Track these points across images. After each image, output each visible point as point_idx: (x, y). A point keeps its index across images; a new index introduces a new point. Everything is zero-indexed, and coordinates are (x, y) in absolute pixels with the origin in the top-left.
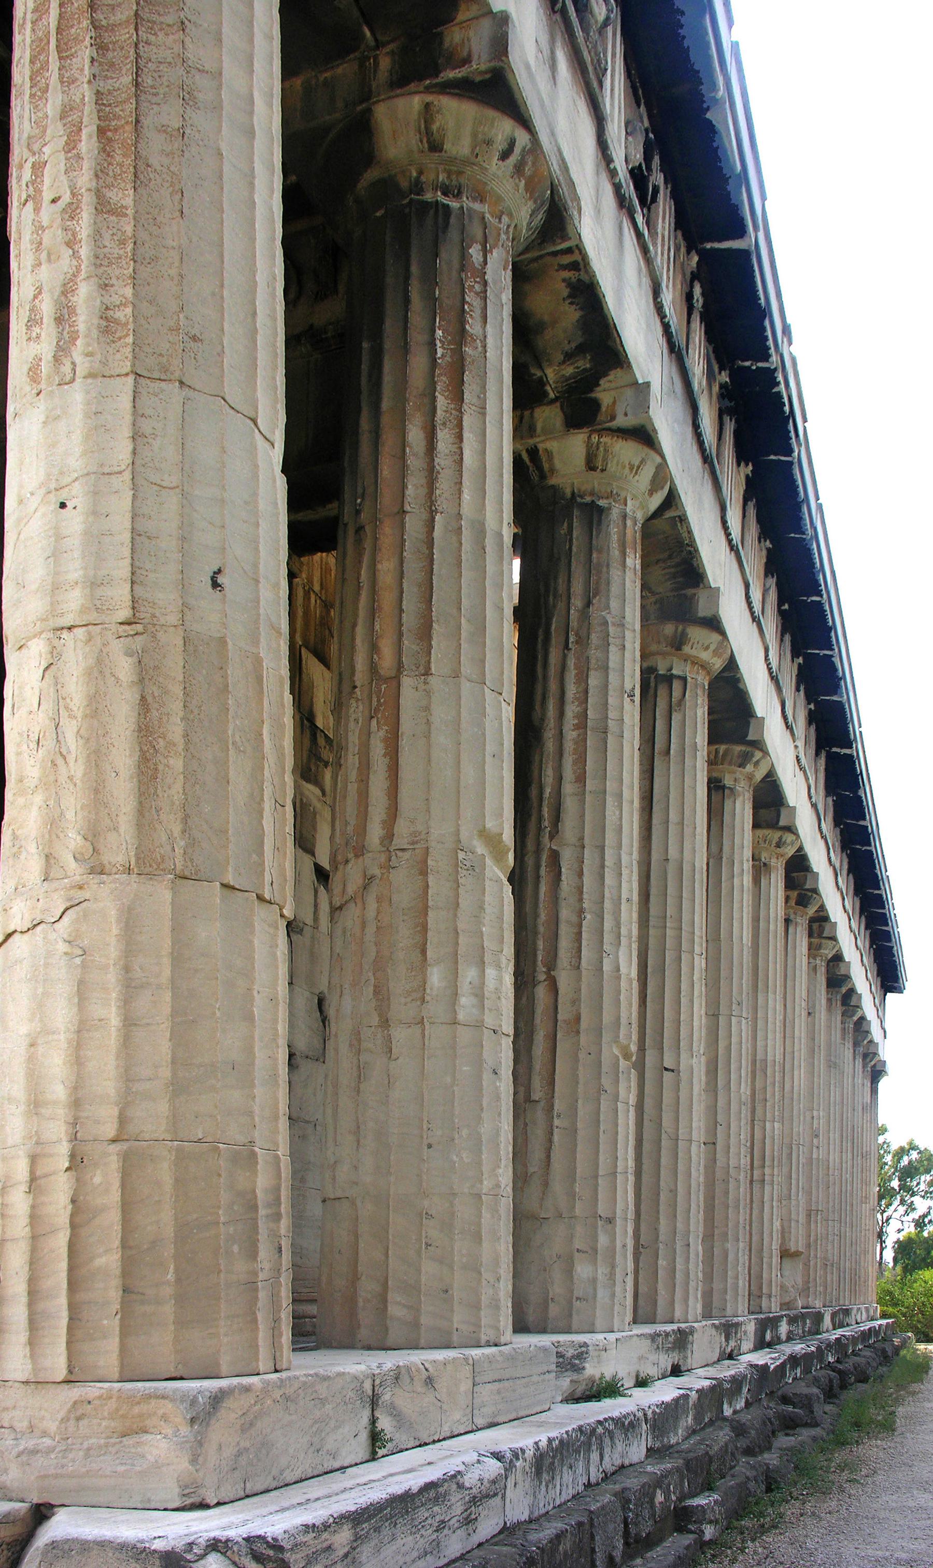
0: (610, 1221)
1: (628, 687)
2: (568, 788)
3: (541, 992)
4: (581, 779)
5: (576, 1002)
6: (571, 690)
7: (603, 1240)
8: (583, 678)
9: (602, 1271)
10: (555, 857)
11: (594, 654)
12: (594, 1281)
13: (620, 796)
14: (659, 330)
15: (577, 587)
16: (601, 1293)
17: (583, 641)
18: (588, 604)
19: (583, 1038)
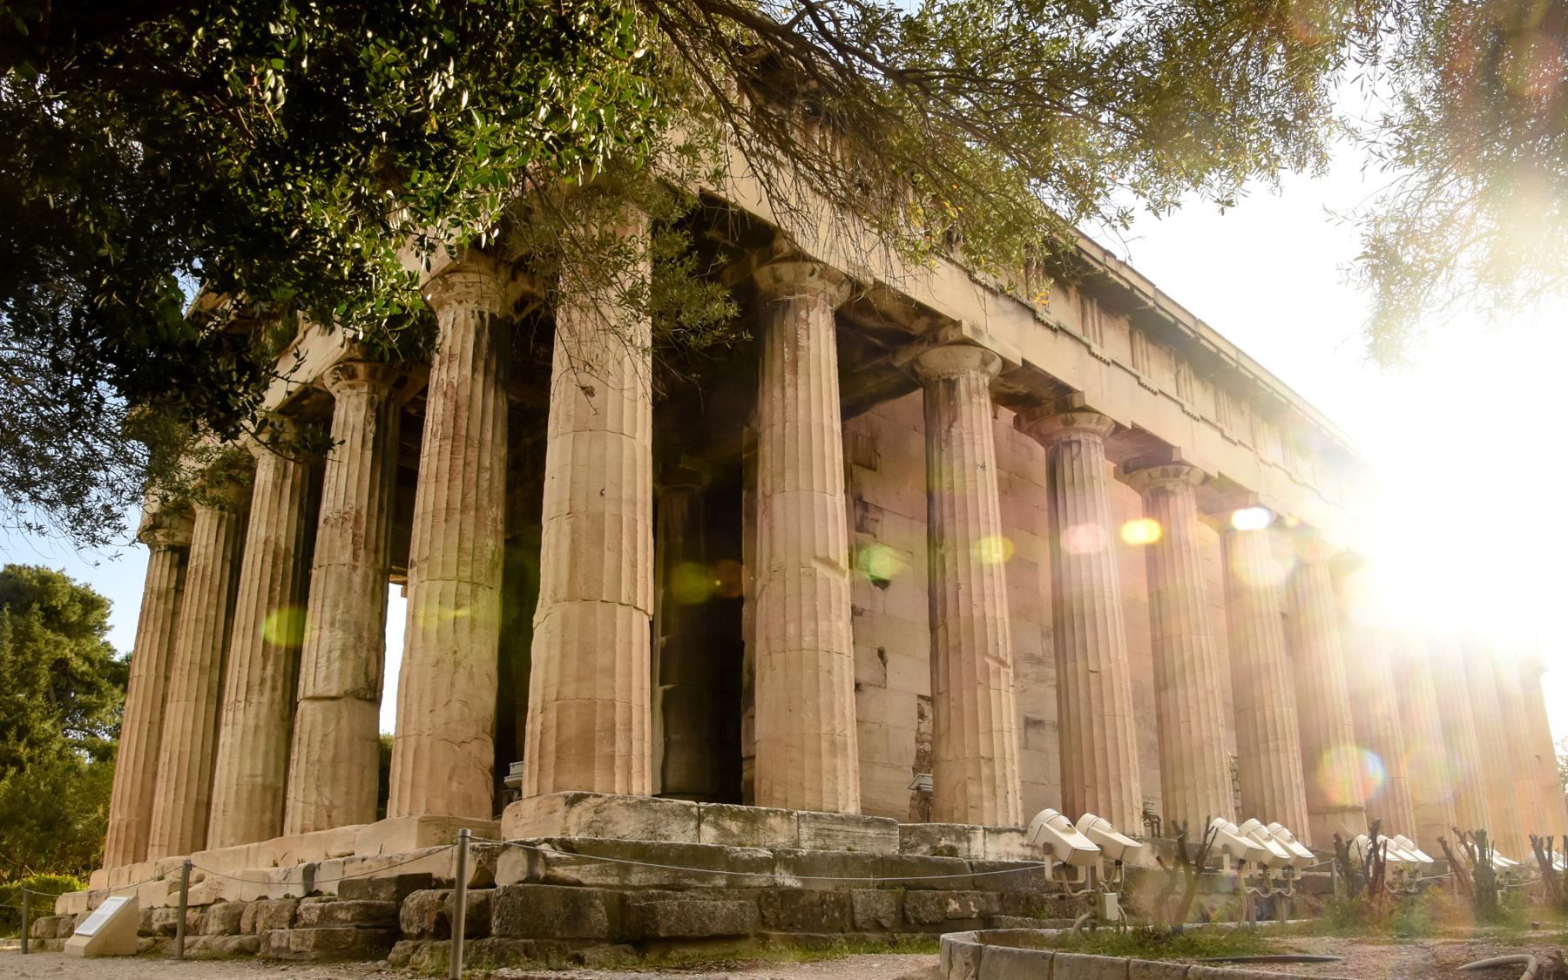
0: (991, 759)
1: (980, 462)
2: (946, 521)
3: (941, 631)
4: (953, 515)
5: (958, 635)
6: (945, 470)
7: (985, 771)
8: (950, 463)
9: (986, 791)
10: (943, 557)
11: (955, 450)
12: (981, 797)
13: (978, 520)
14: (980, 290)
15: (945, 419)
16: (987, 804)
17: (949, 443)
18: (950, 426)
19: (964, 655)
